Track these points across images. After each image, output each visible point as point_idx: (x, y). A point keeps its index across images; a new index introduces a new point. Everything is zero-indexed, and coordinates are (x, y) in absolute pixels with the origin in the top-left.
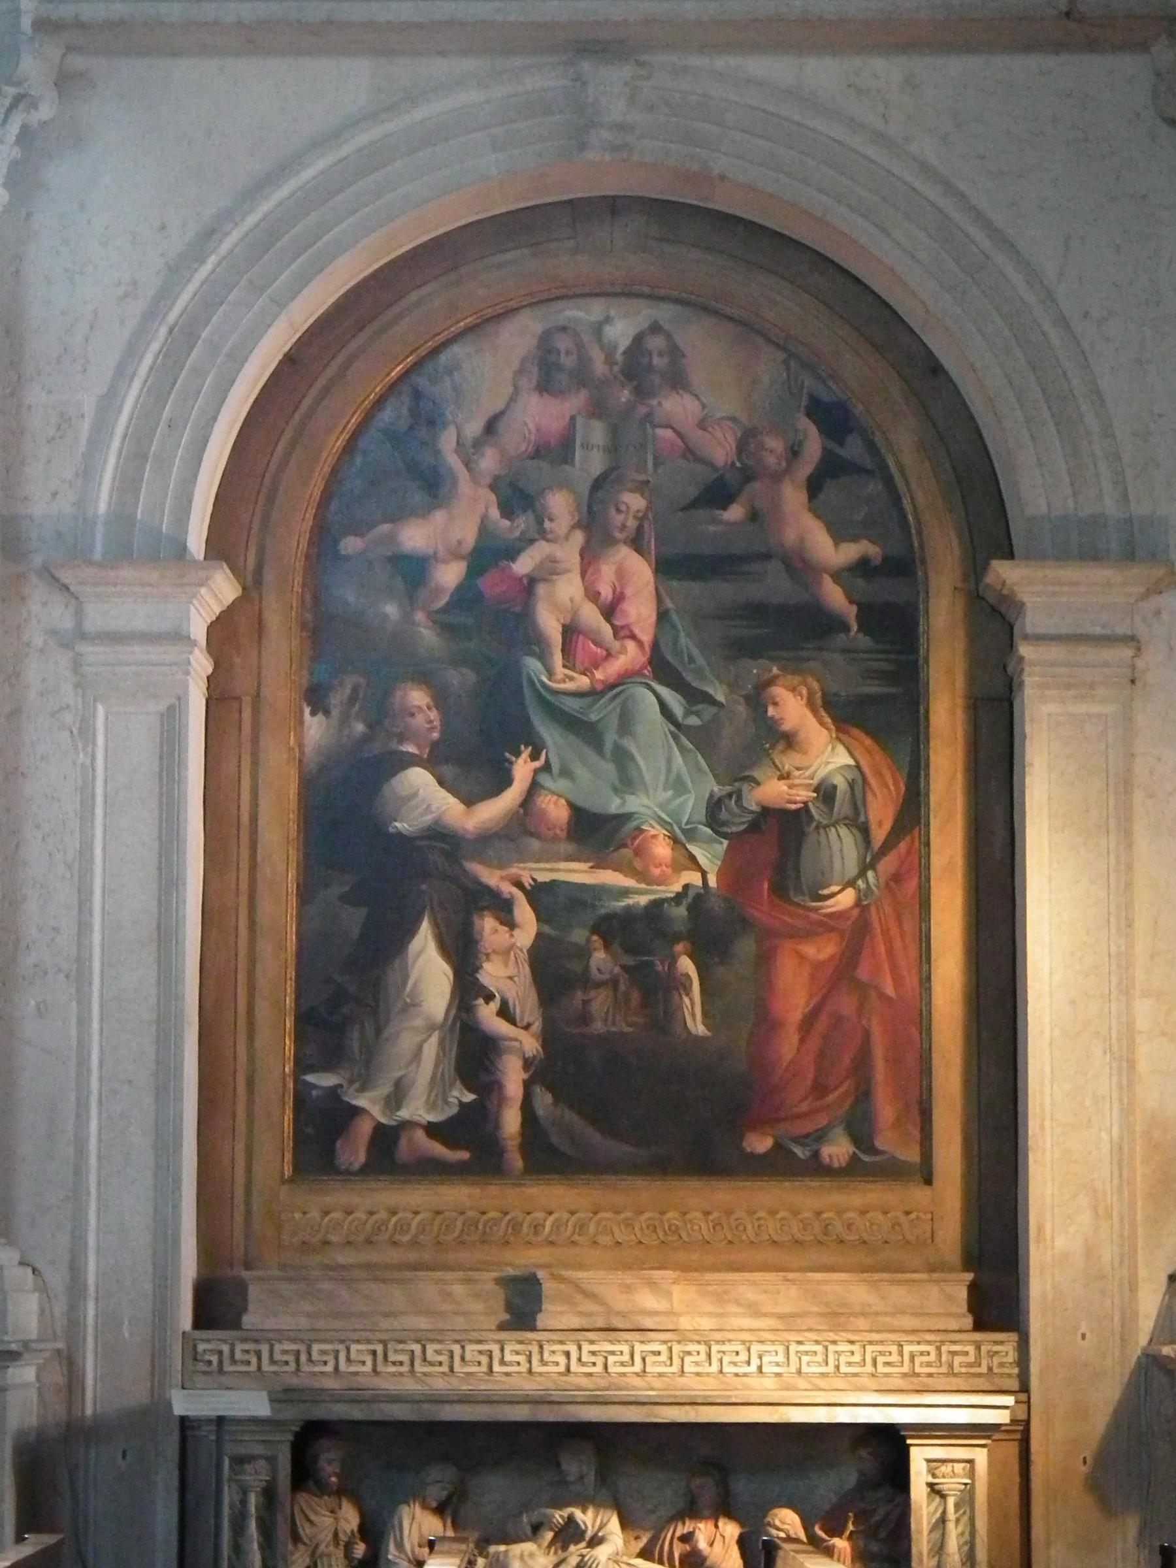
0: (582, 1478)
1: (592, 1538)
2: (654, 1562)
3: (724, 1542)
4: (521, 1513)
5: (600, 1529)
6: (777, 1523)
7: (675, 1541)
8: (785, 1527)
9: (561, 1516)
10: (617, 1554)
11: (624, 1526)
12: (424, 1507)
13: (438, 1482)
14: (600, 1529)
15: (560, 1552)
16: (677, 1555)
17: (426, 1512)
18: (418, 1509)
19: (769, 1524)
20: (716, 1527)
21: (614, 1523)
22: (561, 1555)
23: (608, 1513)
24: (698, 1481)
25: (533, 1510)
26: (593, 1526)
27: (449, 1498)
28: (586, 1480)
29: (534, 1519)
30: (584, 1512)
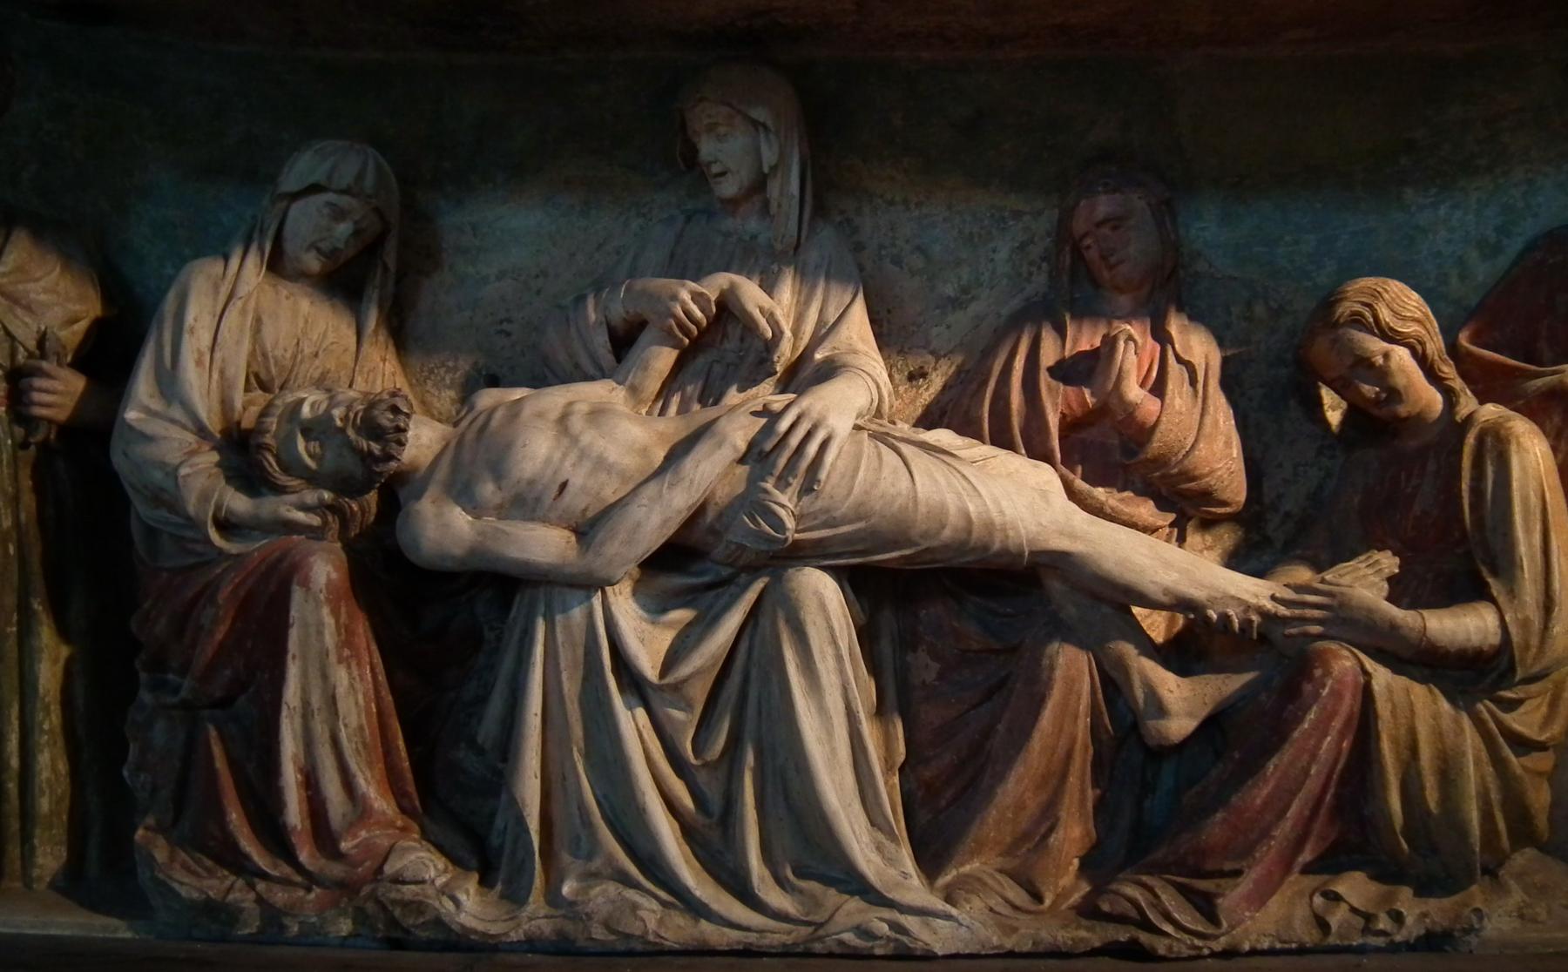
0: (759, 185)
1: (794, 368)
2: (979, 437)
3: (1193, 382)
4: (580, 299)
5: (817, 340)
6: (1385, 315)
7: (1044, 377)
8: (1410, 329)
9: (697, 297)
10: (879, 413)
11: (887, 335)
12: (276, 265)
13: (315, 189)
14: (817, 340)
15: (696, 407)
16: (1053, 421)
17: (285, 289)
18: (251, 271)
19: (1357, 321)
20: (1161, 336)
21: (857, 330)
22: (700, 415)
23: (839, 296)
24: (1104, 205)
25: (616, 286)
26: (796, 332)
27: (369, 250)
28: (774, 189)
29: (618, 312)
30: (769, 287)
